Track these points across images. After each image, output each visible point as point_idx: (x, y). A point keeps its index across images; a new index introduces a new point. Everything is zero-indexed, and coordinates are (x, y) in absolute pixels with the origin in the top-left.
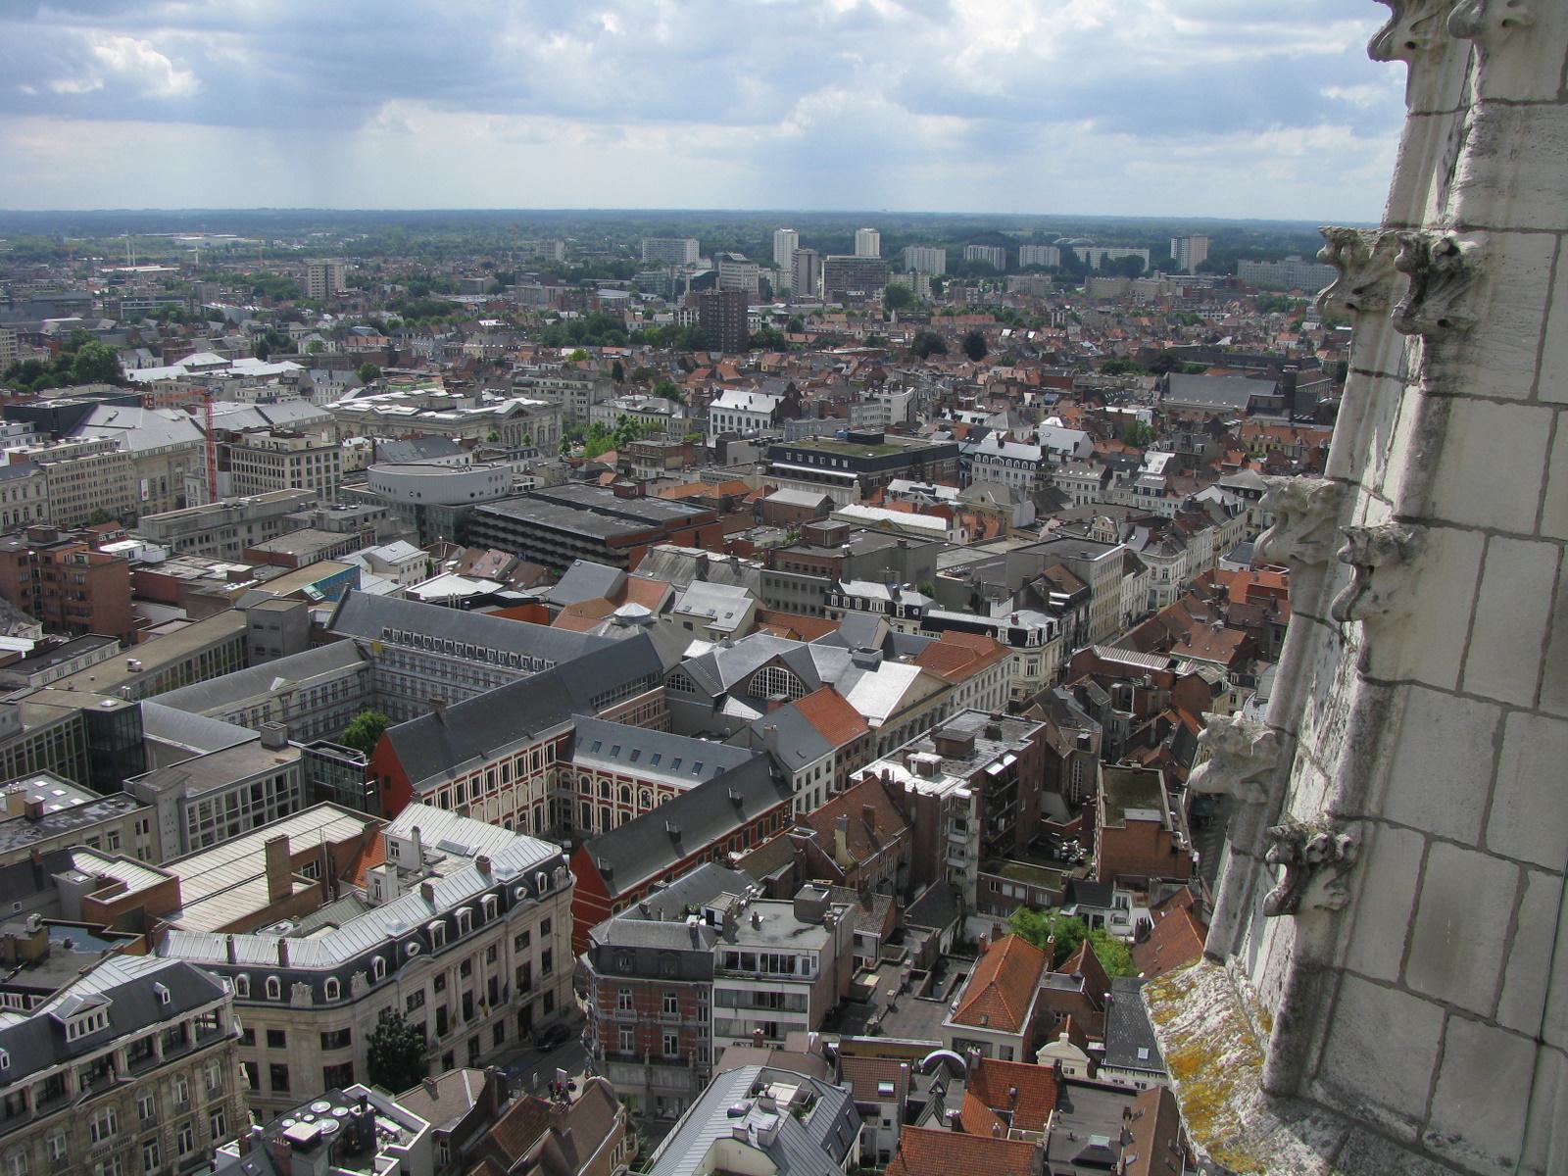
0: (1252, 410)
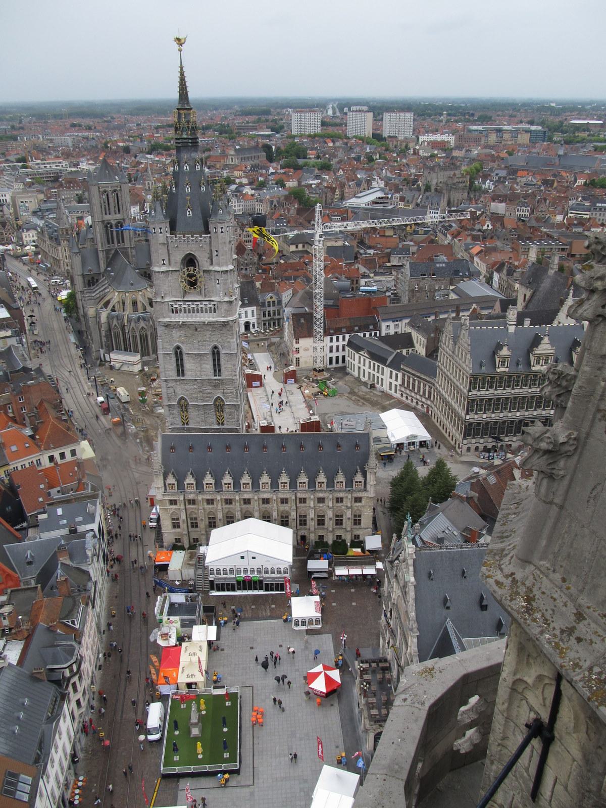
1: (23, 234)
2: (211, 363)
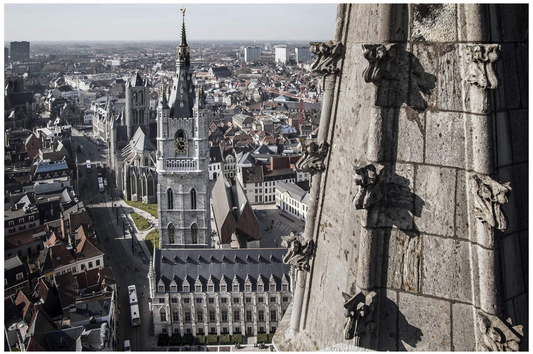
1: (85, 116)
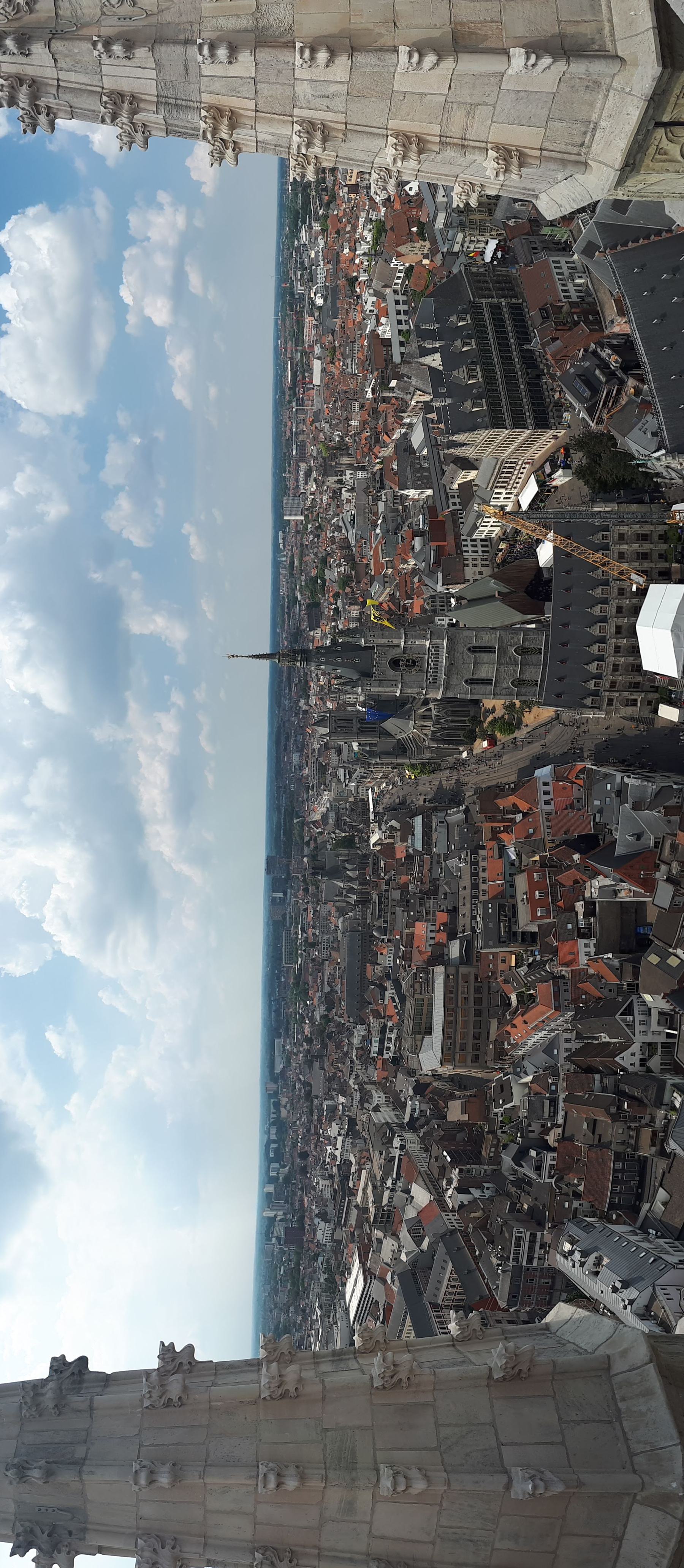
0: (323, 1069)
2: (483, 655)
